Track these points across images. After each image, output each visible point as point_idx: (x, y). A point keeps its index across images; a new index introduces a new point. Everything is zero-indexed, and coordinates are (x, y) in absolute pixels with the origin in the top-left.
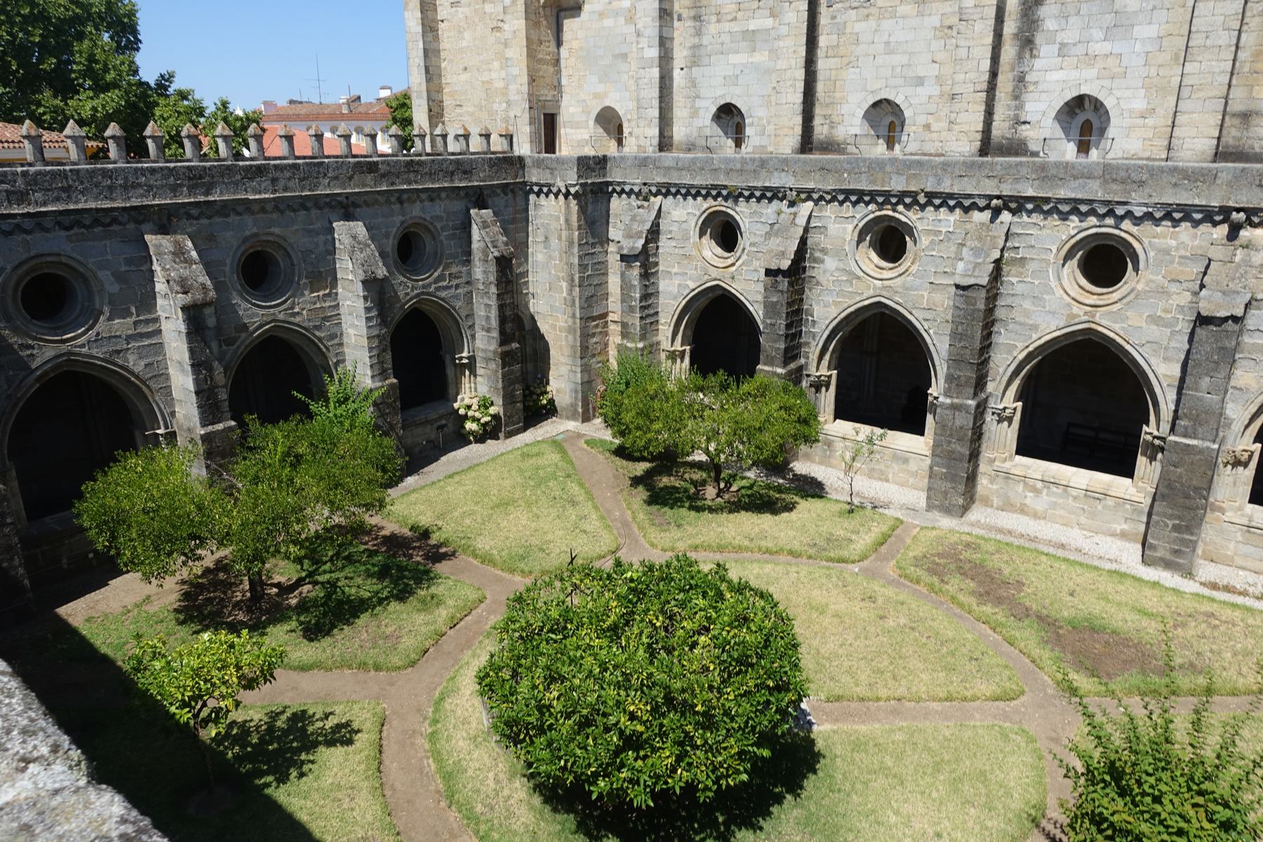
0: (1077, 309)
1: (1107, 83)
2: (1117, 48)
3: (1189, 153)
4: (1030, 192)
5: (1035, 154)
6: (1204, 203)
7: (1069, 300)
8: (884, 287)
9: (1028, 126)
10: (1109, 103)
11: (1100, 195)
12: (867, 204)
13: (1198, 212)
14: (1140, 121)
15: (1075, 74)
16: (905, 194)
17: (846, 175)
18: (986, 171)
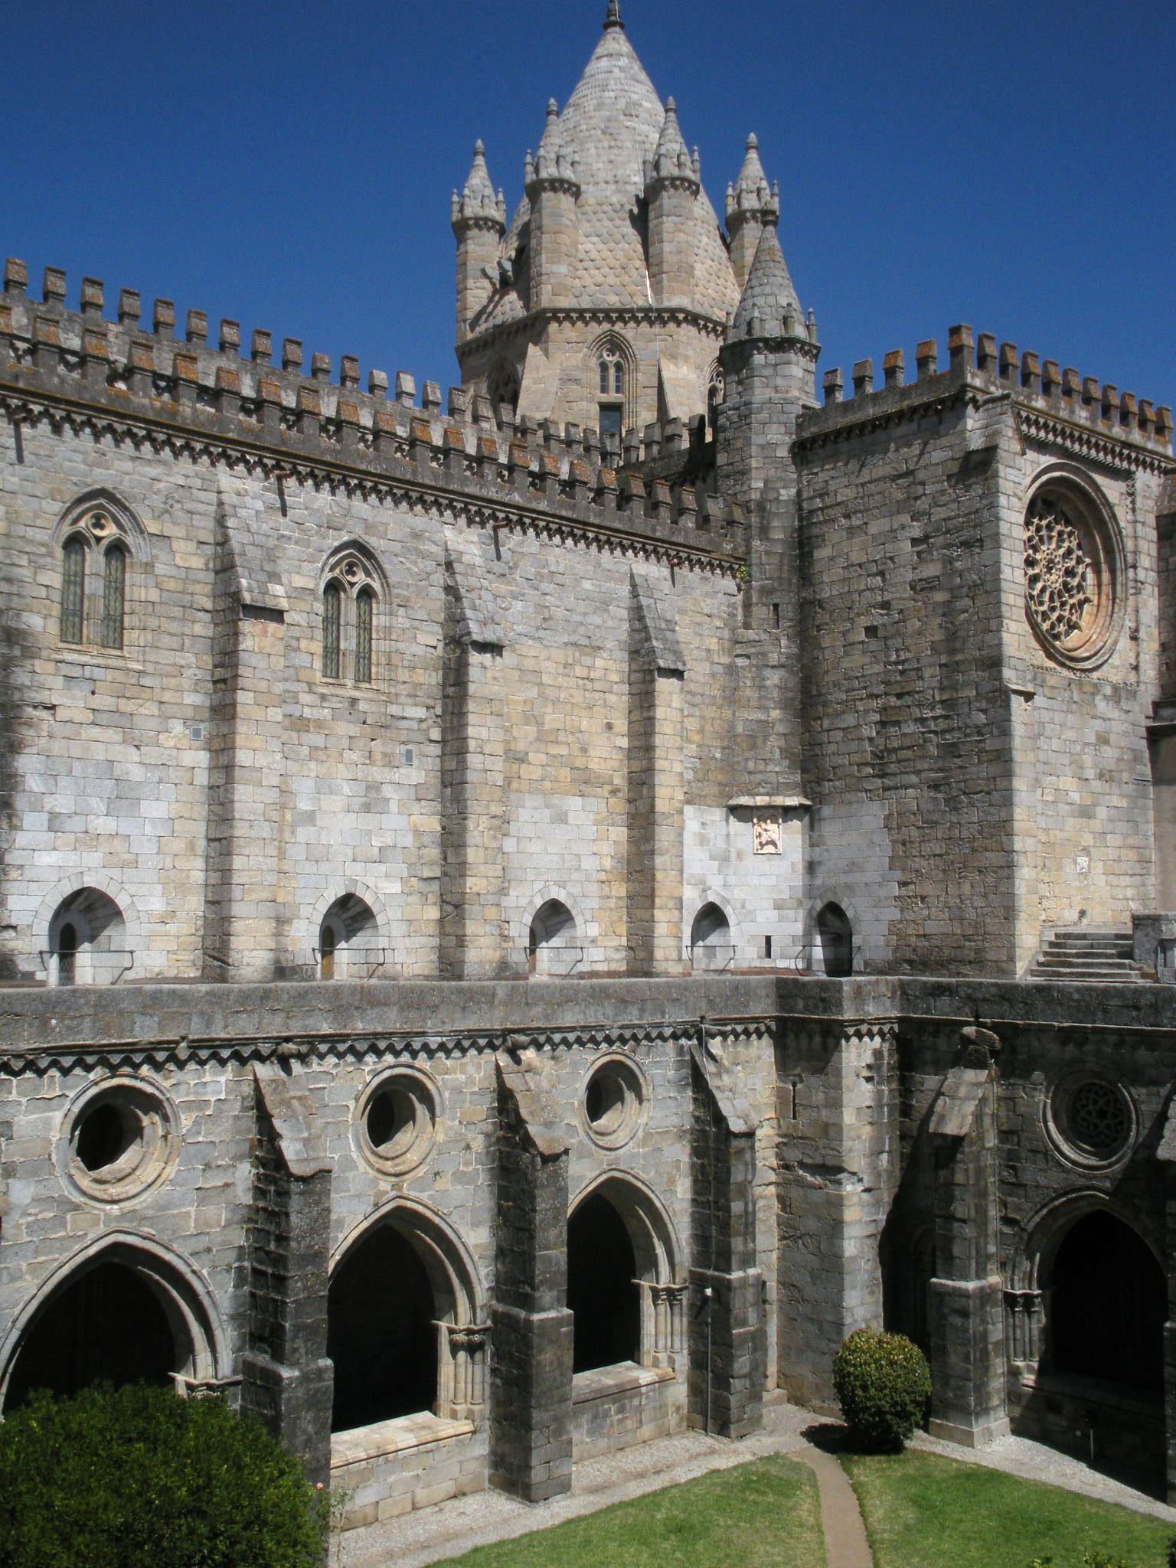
0: (385, 1185)
1: (116, 873)
2: (125, 826)
3: (250, 969)
4: (326, 1029)
5: (29, 976)
6: (488, 1026)
7: (372, 1173)
8: (124, 1215)
9: (12, 933)
10: (122, 901)
11: (399, 1027)
12: (89, 1069)
13: (483, 1037)
14: (161, 928)
15: (72, 858)
16: (157, 1046)
17: (54, 1022)
18: (270, 1003)
